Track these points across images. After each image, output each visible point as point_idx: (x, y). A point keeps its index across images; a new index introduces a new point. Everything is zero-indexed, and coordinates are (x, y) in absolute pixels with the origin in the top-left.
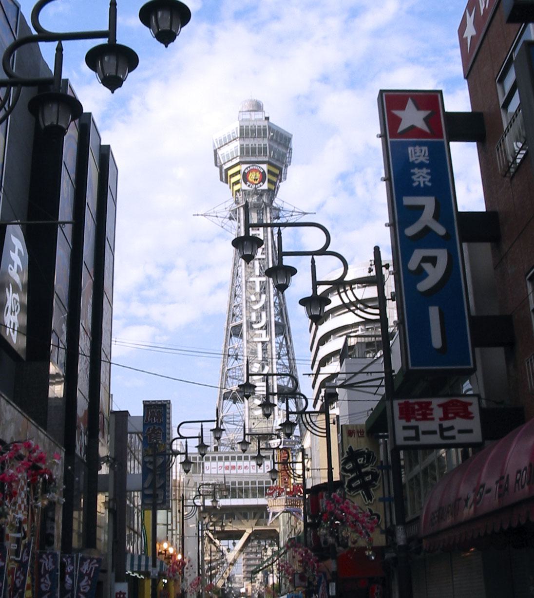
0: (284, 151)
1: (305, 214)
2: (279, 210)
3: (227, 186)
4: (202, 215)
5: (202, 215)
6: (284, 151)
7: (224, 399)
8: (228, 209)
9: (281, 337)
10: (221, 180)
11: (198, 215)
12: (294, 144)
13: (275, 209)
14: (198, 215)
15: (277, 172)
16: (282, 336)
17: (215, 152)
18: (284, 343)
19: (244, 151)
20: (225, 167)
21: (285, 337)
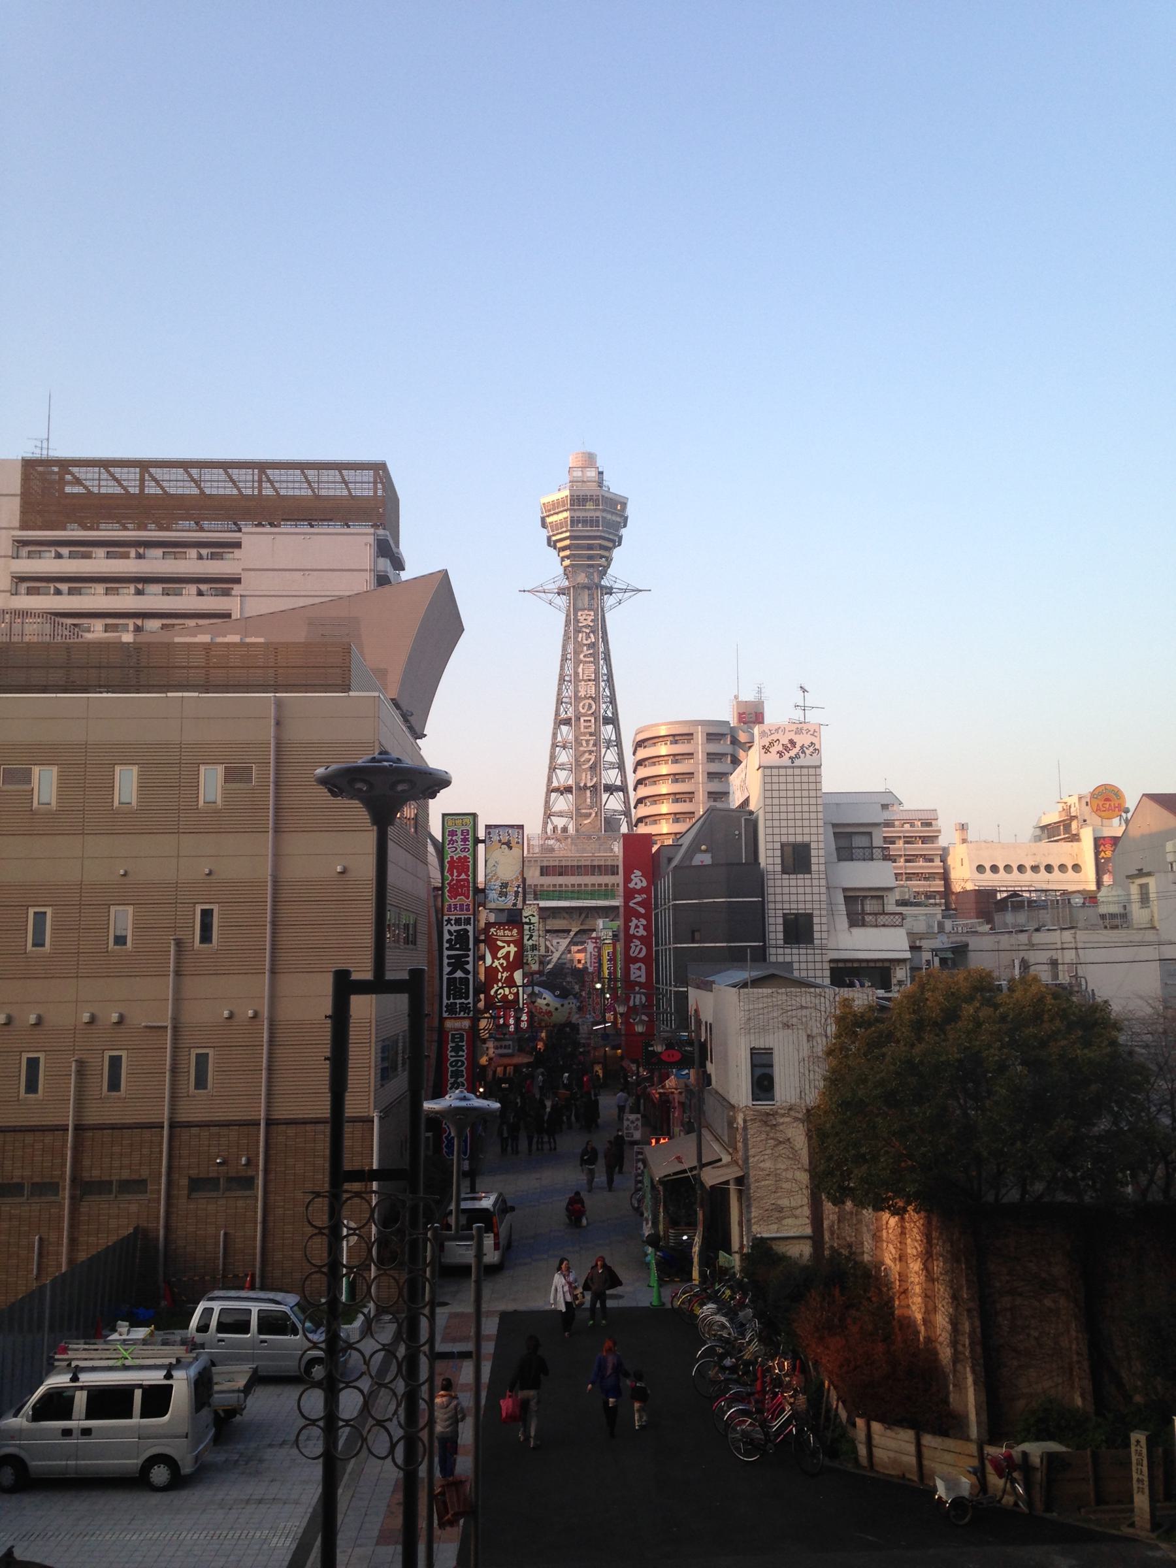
0: (618, 519)
1: (641, 591)
2: (611, 588)
3: (555, 552)
4: (528, 591)
5: (528, 591)
6: (618, 519)
7: (552, 791)
8: (558, 584)
9: (610, 727)
10: (549, 545)
11: (524, 591)
12: (630, 511)
13: (606, 587)
14: (524, 591)
15: (610, 545)
16: (612, 726)
17: (543, 519)
18: (613, 738)
19: (574, 521)
20: (554, 538)
21: (615, 727)
